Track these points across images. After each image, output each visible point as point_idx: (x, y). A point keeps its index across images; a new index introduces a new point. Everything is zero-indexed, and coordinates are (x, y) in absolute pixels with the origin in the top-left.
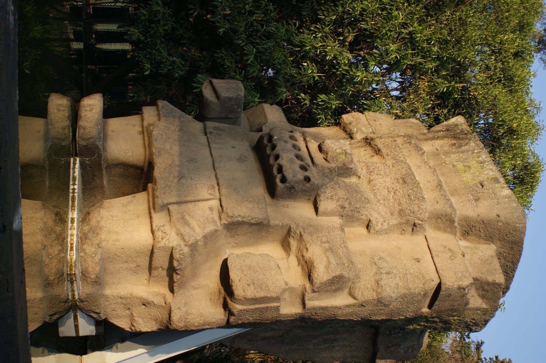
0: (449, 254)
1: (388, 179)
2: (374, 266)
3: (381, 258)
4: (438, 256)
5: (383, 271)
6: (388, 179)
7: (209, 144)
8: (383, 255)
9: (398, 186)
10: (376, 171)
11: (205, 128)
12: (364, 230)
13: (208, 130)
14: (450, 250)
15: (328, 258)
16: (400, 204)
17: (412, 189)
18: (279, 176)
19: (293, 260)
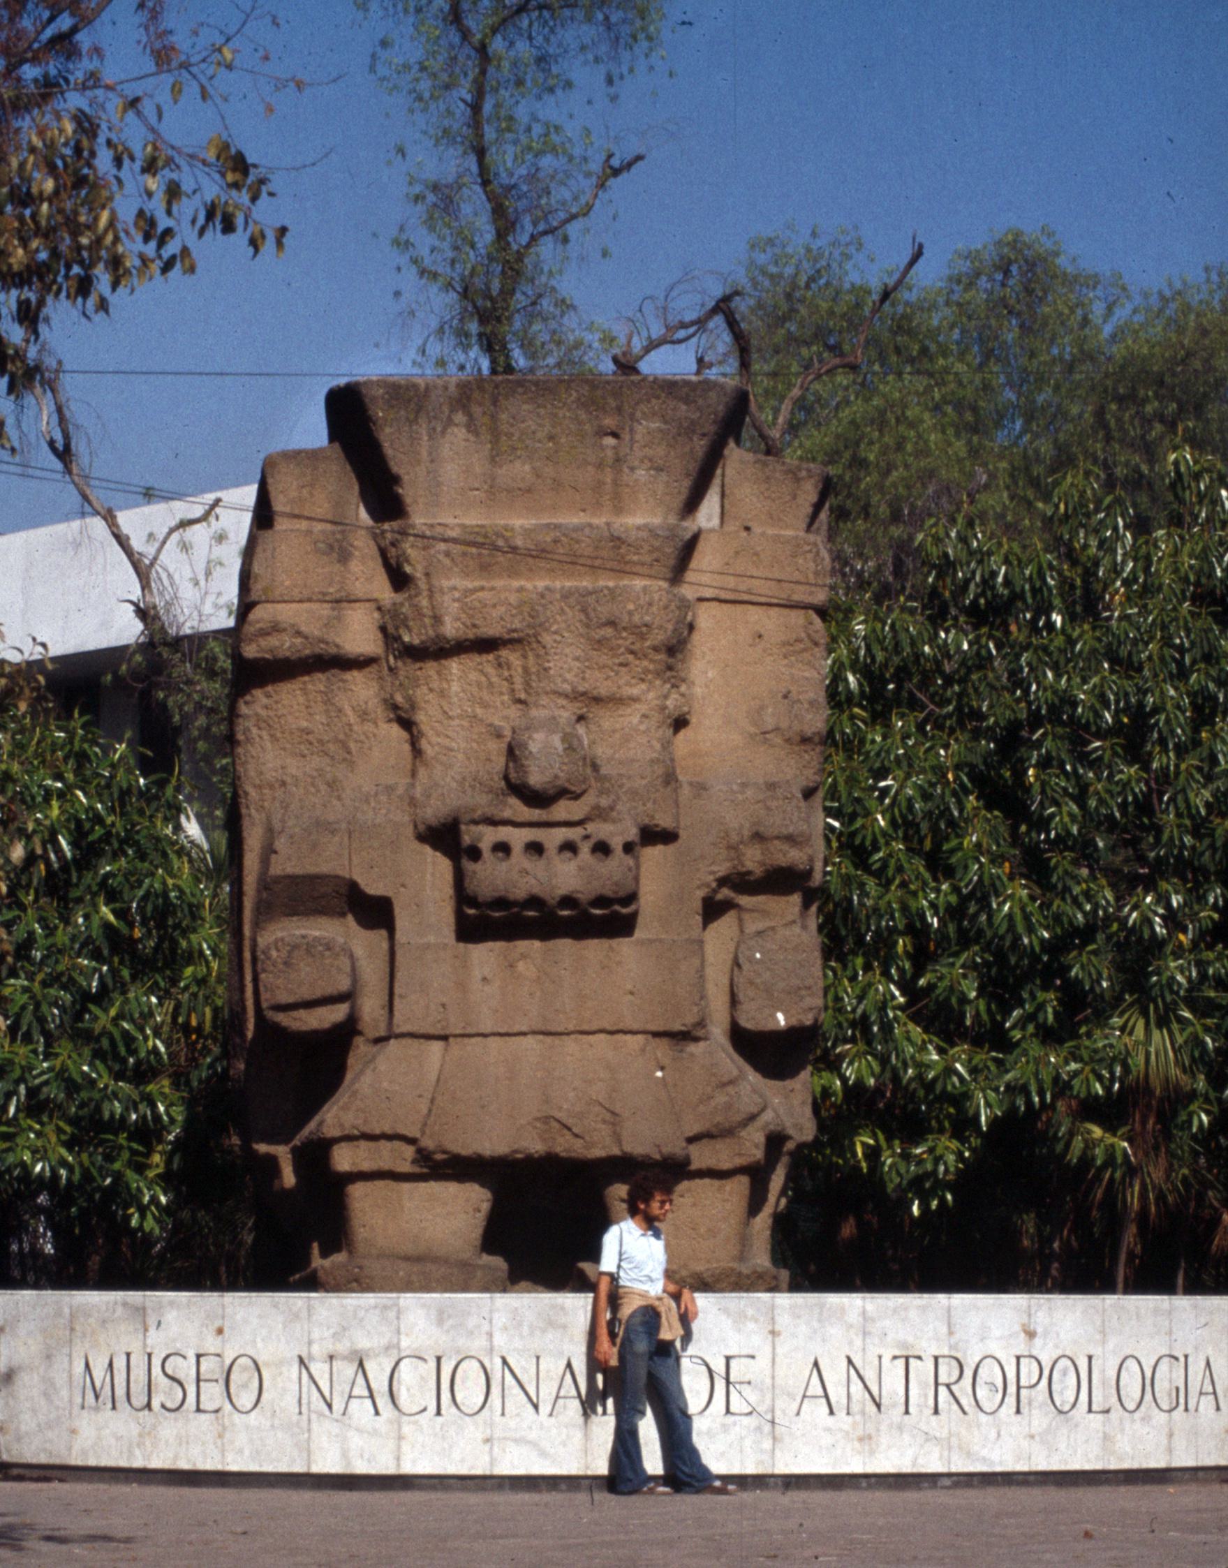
15: (777, 838)
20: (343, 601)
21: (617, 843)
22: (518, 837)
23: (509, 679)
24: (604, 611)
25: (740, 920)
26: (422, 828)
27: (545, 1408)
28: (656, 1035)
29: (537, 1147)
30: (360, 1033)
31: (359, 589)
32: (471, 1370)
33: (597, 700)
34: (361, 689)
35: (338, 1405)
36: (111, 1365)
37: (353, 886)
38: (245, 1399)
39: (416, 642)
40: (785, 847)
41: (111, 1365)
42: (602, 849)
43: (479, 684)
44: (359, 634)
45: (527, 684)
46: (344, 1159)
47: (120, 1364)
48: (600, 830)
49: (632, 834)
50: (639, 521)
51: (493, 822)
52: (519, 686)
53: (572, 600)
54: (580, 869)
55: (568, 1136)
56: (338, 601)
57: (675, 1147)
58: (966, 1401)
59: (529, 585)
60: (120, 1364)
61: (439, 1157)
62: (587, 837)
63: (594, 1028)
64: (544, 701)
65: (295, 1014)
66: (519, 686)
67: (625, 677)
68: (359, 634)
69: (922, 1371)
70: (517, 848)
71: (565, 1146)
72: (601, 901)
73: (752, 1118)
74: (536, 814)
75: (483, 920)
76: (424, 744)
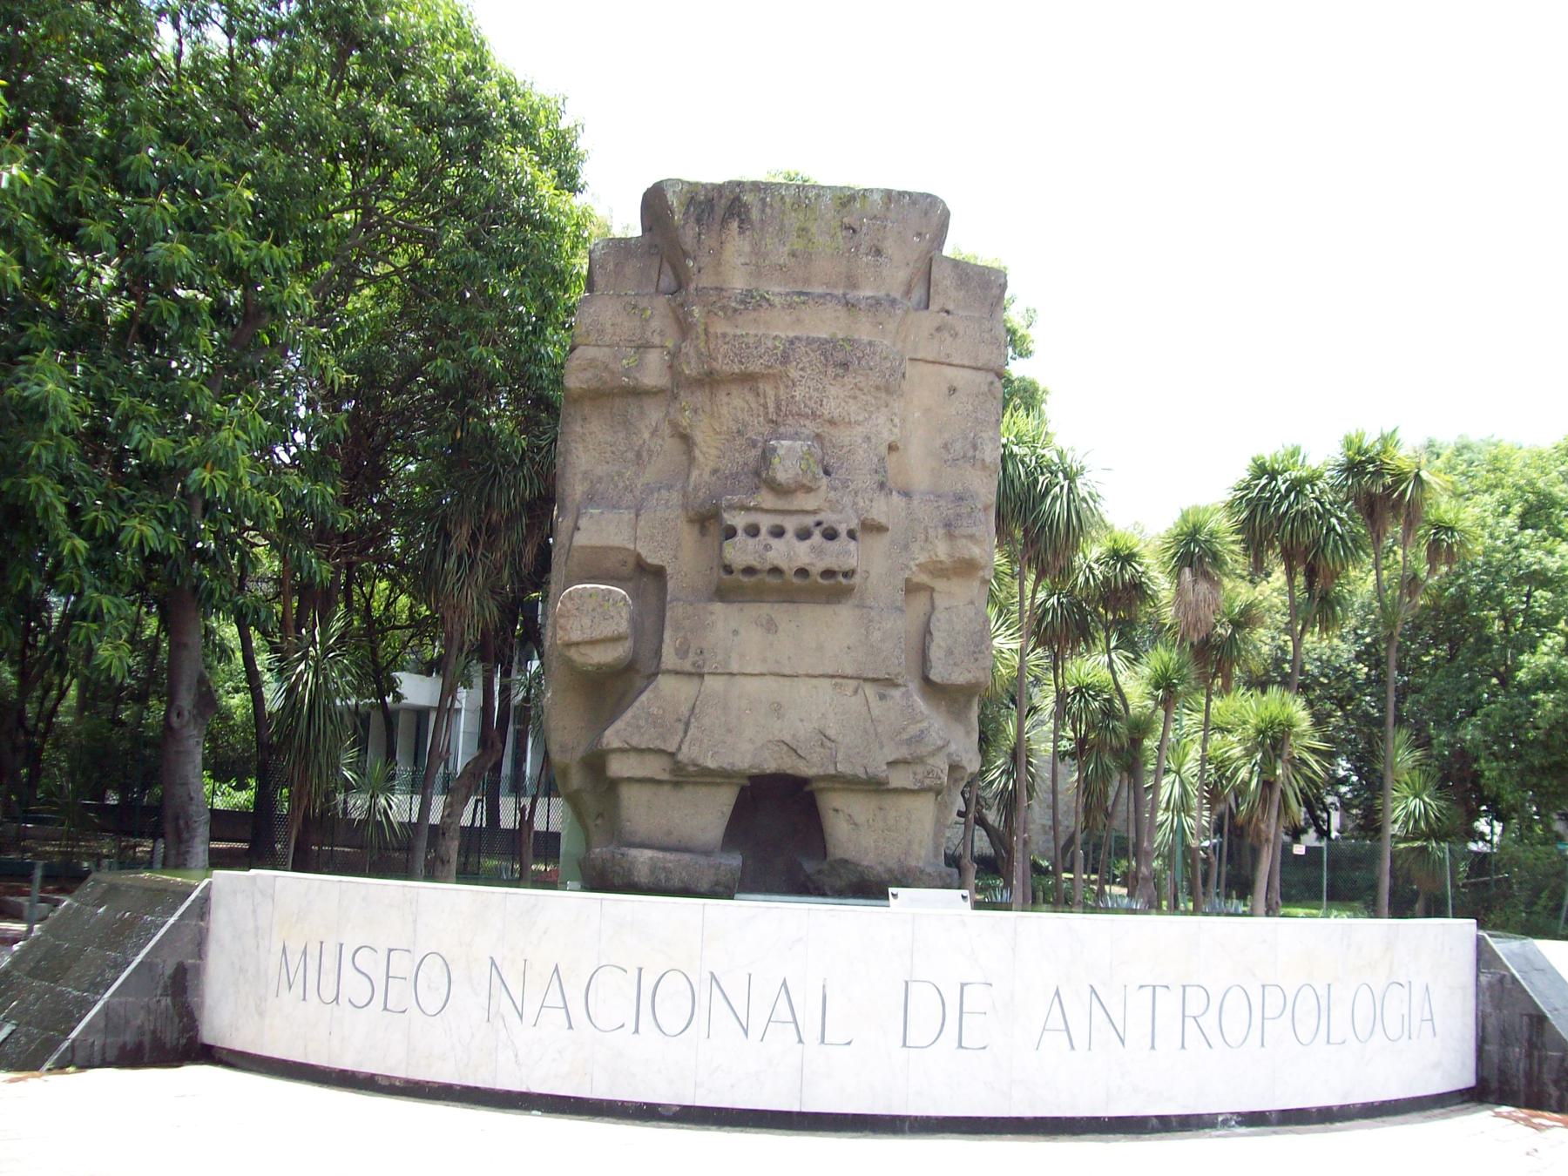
0: (946, 335)
1: (833, 391)
2: (960, 462)
3: (945, 446)
4: (948, 356)
5: (971, 453)
6: (833, 391)
7: (731, 674)
8: (939, 442)
9: (849, 380)
10: (811, 404)
11: (677, 673)
12: (894, 456)
13: (687, 666)
14: (938, 329)
16: (878, 388)
17: (859, 359)
18: (841, 579)
19: (940, 585)
20: (643, 347)
21: (843, 529)
22: (766, 522)
23: (765, 406)
24: (840, 356)
25: (932, 598)
26: (691, 513)
27: (755, 1032)
28: (866, 680)
29: (771, 766)
30: (638, 671)
31: (656, 340)
32: (673, 983)
33: (832, 422)
34: (654, 413)
35: (530, 1011)
36: (305, 953)
37: (639, 555)
38: (432, 1002)
39: (694, 373)
40: (970, 545)
41: (305, 953)
42: (831, 535)
43: (742, 410)
44: (653, 372)
45: (778, 408)
46: (618, 767)
47: (313, 951)
48: (829, 518)
49: (854, 524)
50: (869, 293)
51: (748, 509)
52: (771, 410)
53: (815, 346)
54: (813, 548)
55: (794, 757)
56: (638, 347)
57: (879, 768)
58: (1215, 1038)
59: (783, 335)
60: (313, 951)
61: (691, 769)
62: (819, 524)
63: (818, 672)
64: (790, 420)
65: (583, 649)
66: (771, 410)
67: (853, 407)
68: (653, 372)
69: (1168, 1004)
70: (764, 530)
71: (791, 765)
72: (828, 573)
73: (940, 749)
74: (781, 504)
75: (735, 586)
76: (697, 453)
